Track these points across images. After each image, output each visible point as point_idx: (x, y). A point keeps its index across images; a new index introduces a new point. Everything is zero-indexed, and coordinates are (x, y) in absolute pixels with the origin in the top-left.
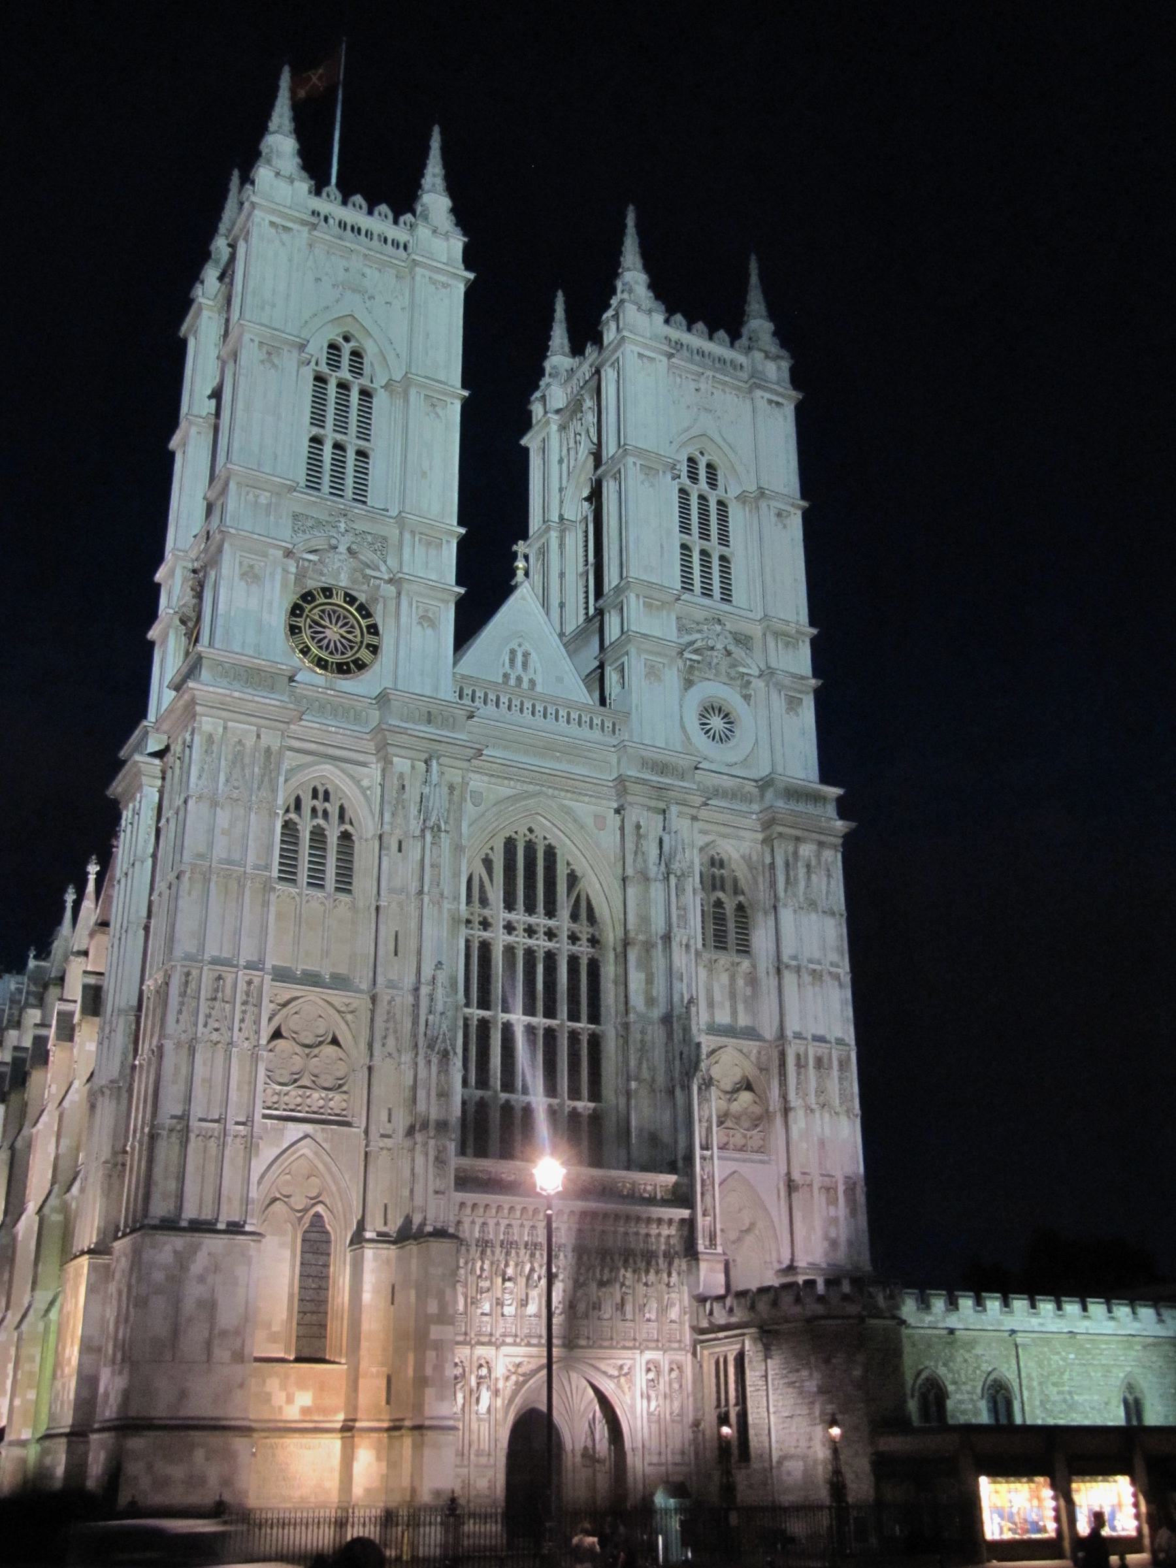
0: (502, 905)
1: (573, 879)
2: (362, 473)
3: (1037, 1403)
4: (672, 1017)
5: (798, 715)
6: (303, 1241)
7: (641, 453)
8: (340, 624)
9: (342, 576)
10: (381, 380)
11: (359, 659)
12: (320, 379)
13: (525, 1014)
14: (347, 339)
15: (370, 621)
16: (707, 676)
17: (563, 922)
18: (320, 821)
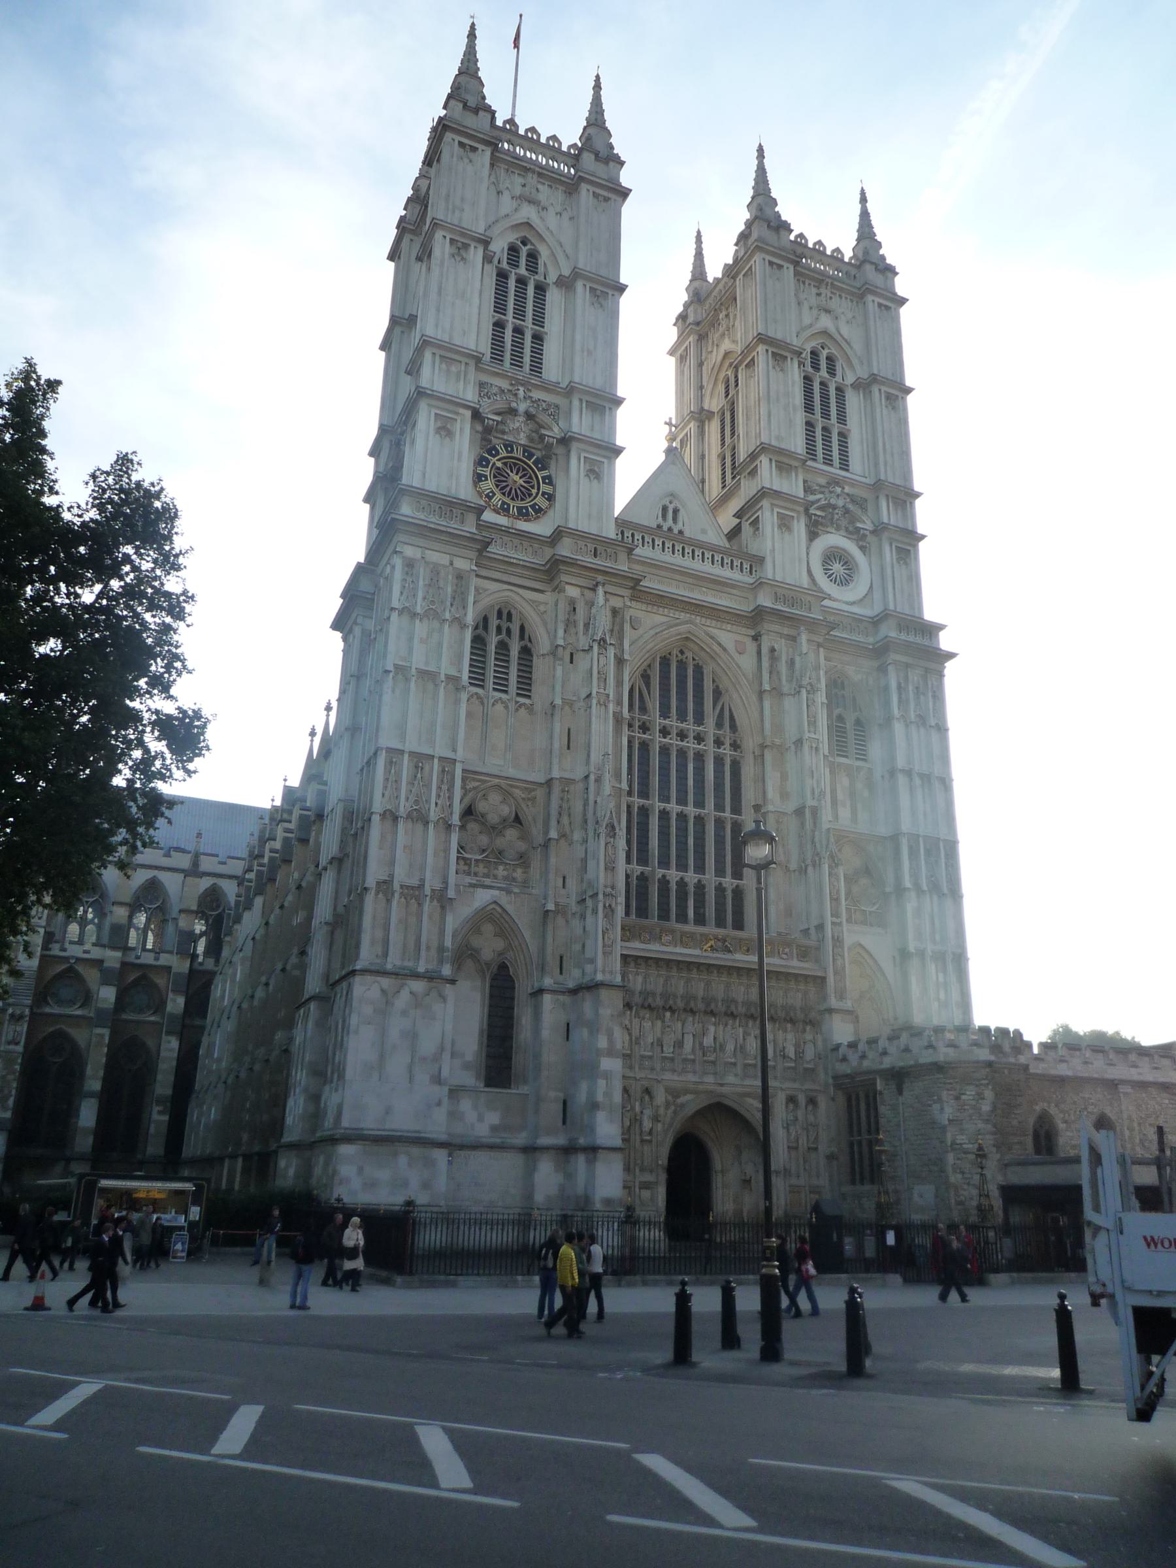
0: (658, 713)
1: (717, 693)
2: (537, 352)
3: (1137, 1141)
4: (804, 807)
5: (906, 564)
6: (491, 986)
8: (520, 475)
9: (522, 434)
10: (552, 278)
11: (536, 504)
12: (502, 276)
13: (677, 804)
14: (524, 243)
15: (545, 473)
16: (829, 529)
17: (709, 727)
18: (503, 636)
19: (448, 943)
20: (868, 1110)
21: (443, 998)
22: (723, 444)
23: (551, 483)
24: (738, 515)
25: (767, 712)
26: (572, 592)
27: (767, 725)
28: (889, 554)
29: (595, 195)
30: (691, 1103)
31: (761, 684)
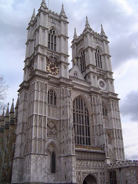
2: (55, 48)
7: (90, 48)
10: (57, 36)
12: (49, 34)
15: (57, 67)
19: (46, 148)
20: (114, 175)
21: (46, 158)
22: (81, 62)
23: (58, 69)
24: (86, 75)
25: (93, 108)
26: (63, 88)
27: (93, 110)
28: (109, 82)
29: (64, 23)
30: (86, 175)
31: (92, 103)
